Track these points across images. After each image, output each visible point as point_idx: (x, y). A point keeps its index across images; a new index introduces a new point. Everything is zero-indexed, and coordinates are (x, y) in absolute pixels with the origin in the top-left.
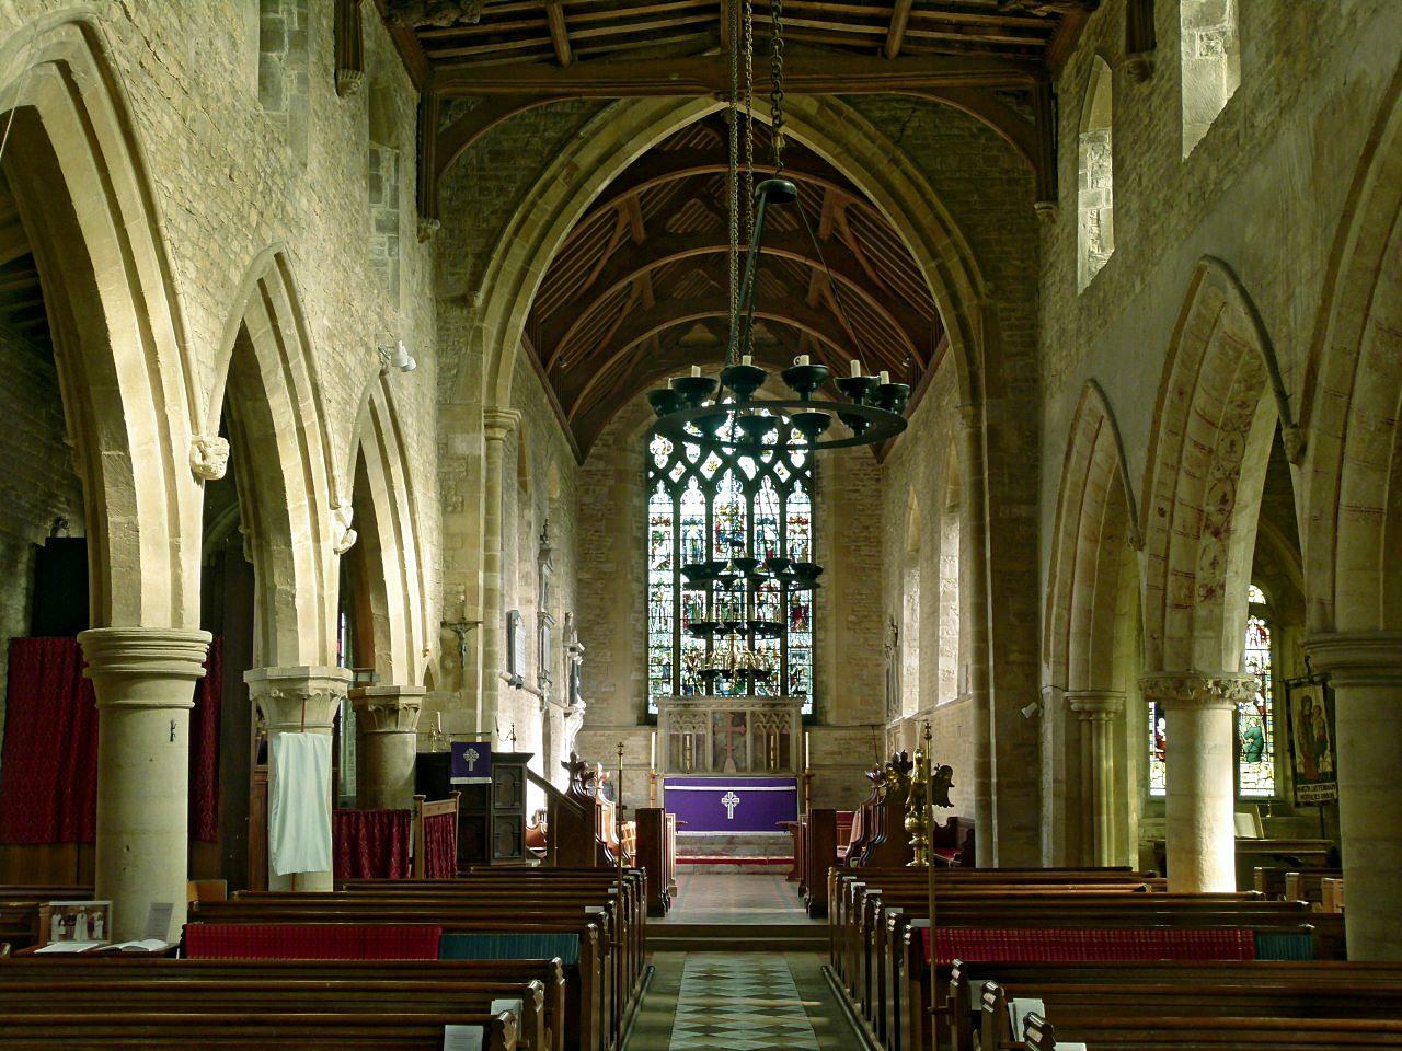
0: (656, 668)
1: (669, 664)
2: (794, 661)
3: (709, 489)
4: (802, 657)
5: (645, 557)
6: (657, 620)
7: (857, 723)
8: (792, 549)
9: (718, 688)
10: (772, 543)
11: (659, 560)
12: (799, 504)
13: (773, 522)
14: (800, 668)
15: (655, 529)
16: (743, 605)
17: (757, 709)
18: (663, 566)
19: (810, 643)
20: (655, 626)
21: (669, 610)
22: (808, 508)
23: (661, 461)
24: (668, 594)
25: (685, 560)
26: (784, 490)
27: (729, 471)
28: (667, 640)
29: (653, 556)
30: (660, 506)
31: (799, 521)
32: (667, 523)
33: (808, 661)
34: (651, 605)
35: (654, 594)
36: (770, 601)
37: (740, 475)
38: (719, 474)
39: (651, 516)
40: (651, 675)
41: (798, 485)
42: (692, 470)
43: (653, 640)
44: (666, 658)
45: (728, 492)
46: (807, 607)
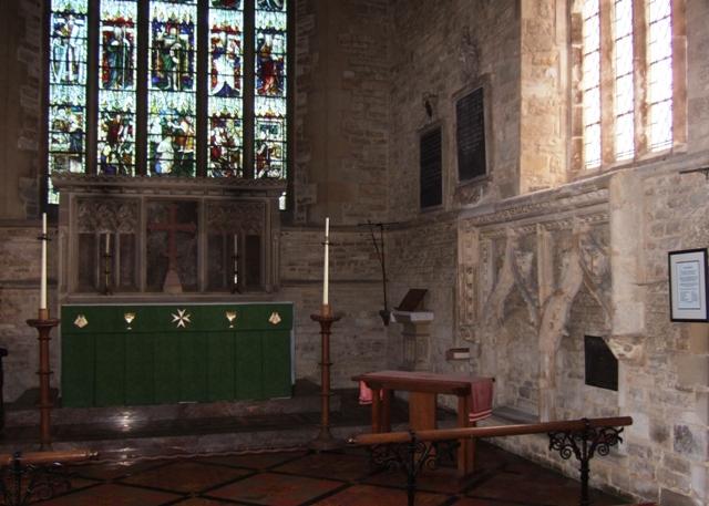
0: (59, 137)
1: (79, 131)
2: (262, 136)
4: (273, 131)
6: (63, 65)
7: (354, 222)
14: (270, 145)
16: (191, 52)
17: (213, 196)
19: (284, 113)
20: (58, 74)
21: (82, 52)
24: (80, 29)
28: (77, 95)
33: (280, 136)
34: (54, 42)
35: (58, 27)
36: (230, 49)
40: (53, 146)
43: (56, 95)
44: (76, 122)
46: (280, 63)
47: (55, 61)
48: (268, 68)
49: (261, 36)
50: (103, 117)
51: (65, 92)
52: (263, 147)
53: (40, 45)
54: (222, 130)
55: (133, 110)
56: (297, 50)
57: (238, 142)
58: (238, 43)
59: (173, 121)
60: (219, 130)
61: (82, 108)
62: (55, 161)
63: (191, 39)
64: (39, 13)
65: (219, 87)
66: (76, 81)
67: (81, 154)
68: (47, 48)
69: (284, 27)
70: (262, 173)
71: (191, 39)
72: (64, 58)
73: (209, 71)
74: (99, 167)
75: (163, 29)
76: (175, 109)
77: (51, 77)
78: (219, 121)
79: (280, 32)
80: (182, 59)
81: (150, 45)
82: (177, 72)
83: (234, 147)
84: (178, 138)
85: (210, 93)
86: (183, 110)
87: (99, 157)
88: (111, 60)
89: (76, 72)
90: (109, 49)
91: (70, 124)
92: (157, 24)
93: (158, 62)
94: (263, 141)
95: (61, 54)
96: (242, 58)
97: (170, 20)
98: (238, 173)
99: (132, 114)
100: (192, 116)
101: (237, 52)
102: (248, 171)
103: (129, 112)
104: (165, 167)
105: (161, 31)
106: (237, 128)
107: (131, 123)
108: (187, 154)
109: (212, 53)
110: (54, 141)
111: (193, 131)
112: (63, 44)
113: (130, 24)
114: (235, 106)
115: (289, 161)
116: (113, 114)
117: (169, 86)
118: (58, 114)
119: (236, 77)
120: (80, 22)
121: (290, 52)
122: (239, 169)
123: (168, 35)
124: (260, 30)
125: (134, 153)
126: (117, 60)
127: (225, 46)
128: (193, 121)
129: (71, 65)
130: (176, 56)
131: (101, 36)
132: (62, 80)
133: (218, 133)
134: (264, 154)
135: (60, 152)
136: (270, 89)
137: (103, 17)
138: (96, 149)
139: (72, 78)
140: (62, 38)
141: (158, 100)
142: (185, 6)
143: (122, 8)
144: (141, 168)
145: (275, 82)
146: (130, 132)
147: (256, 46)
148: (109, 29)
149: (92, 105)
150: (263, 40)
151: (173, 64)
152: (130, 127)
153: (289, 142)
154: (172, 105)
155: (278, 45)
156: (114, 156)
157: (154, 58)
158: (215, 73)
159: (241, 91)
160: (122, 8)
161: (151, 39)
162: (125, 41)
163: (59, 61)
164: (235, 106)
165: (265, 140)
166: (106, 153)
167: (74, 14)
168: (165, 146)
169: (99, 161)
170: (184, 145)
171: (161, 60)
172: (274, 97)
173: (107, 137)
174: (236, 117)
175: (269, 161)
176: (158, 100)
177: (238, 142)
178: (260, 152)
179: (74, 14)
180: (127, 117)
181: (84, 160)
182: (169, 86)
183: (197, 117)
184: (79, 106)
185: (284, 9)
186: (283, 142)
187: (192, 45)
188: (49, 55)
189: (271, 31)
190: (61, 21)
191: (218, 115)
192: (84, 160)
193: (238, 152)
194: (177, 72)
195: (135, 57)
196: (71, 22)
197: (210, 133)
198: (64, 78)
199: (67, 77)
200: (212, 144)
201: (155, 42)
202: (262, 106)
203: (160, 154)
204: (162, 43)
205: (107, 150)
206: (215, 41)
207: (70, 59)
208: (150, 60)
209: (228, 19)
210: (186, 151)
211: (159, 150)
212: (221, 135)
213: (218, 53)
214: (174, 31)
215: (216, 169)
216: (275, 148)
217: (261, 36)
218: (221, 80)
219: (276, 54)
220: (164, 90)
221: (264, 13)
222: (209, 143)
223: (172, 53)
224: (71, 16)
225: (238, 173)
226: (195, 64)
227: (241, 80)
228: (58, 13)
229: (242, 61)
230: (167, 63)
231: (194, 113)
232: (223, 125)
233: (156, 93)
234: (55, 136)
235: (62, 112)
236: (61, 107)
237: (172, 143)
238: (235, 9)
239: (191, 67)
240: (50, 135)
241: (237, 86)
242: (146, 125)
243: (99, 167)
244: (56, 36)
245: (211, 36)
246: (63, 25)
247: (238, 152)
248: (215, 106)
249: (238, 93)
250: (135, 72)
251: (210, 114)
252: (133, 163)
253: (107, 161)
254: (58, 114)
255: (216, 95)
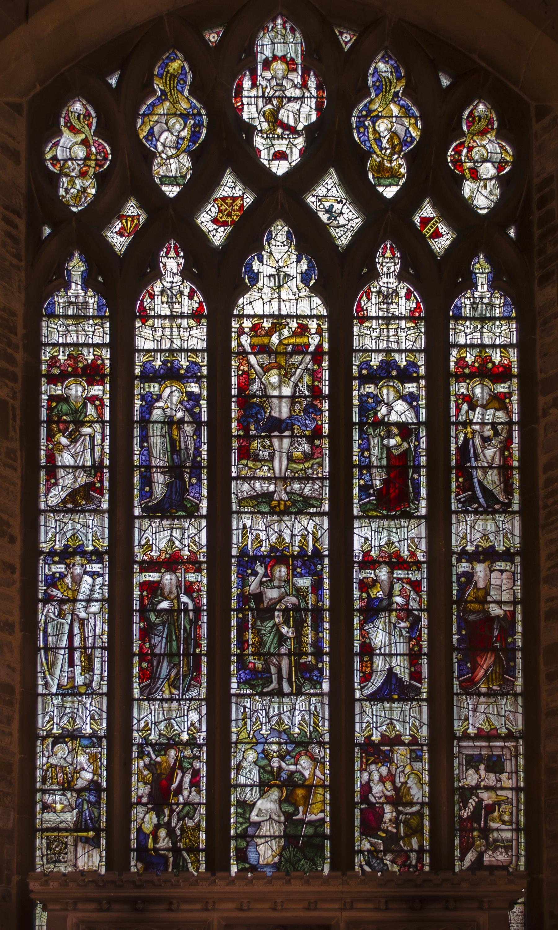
0: (58, 800)
1: (94, 786)
2: (471, 778)
3: (221, 278)
4: (495, 766)
5: (33, 471)
6: (62, 657)
8: (463, 450)
9: (242, 856)
10: (405, 430)
11: (67, 480)
12: (486, 327)
13: (406, 375)
14: (487, 797)
15: (58, 390)
16: (317, 612)
18: (78, 501)
20: (56, 674)
21: (99, 627)
22: (505, 333)
23: (78, 190)
24: (92, 582)
25: (147, 481)
26: (438, 287)
27: (280, 231)
28: (91, 716)
29: (52, 470)
30: (75, 325)
31: (487, 372)
32: (92, 373)
35: (53, 581)
37: (310, 236)
38: (248, 235)
39: (46, 356)
41: (481, 270)
42: (171, 221)
43: (50, 716)
44: (87, 768)
45: (280, 289)
47: (47, 649)
48: (483, 634)
49: (464, 567)
50: (142, 754)
51: (69, 707)
52: (472, 802)
53: (16, 617)
54: (384, 771)
55: (201, 737)
56: (545, 590)
57: (418, 793)
58: (416, 585)
59: (282, 757)
60: (378, 771)
61: (100, 739)
62: (49, 847)
63: (317, 586)
64: (14, 554)
65: (378, 681)
66: (88, 685)
67: (98, 831)
68: (30, 624)
69: (516, 543)
70: (471, 856)
71: (317, 586)
72: (64, 643)
73: (357, 647)
74: (133, 855)
75: (260, 570)
76: (287, 732)
77: (41, 682)
78: (377, 752)
79: (507, 556)
80: (299, 627)
81: (234, 604)
82: (289, 655)
83: (412, 804)
84: (292, 789)
85: (358, 695)
86: (302, 732)
87: (133, 836)
88: (155, 640)
89: (88, 669)
90: (152, 617)
91: (77, 771)
92: (247, 561)
93: (250, 636)
94: (473, 790)
95: (58, 635)
96: (424, 616)
97: (273, 548)
98: (420, 859)
99: (200, 746)
100: (321, 744)
101: (414, 605)
102: (442, 857)
103: (192, 743)
104: (266, 852)
105: (255, 574)
106: (417, 765)
107: (197, 765)
108: (311, 823)
109: (361, 611)
110: (46, 807)
111: (323, 775)
112: (61, 615)
113: (193, 563)
114: (410, 719)
115: (532, 829)
116: (162, 748)
117: (274, 685)
118: (54, 754)
119: (414, 657)
120: (97, 568)
121: (529, 599)
122: (421, 851)
123: (269, 580)
124: (463, 554)
125: (204, 824)
126: (169, 640)
127: (390, 595)
128: (324, 754)
129: (77, 655)
130: (286, 622)
131: (137, 593)
132: (60, 686)
133: (376, 777)
134: (475, 816)
135: (57, 829)
136: (488, 679)
137: (139, 554)
138: (128, 820)
139: (80, 680)
140: (62, 602)
141: (254, 714)
142: (304, 520)
143: (177, 534)
144: (217, 861)
145: (497, 661)
146: (195, 783)
147: (455, 588)
148: (153, 577)
149: (119, 735)
150: (469, 576)
151: (282, 639)
152: (196, 773)
153: (531, 790)
154: (280, 722)
155: (500, 585)
156: (162, 833)
157: (242, 628)
158: (368, 650)
159: (425, 687)
160: (177, 534)
161: (234, 591)
162: (184, 599)
163: (56, 649)
164: (410, 719)
165: (477, 787)
166: (148, 827)
167: (84, 554)
168: (267, 804)
169: (134, 844)
170: (306, 805)
171: (257, 633)
172: (495, 694)
173: (150, 795)
174: (414, 741)
175: (486, 832)
176: (254, 714)
177: (418, 793)
178: (465, 814)
179: (84, 554)
180: (188, 753)
181: (103, 842)
182: (274, 685)
183: (334, 745)
184: (94, 734)
185: (516, 507)
186: (517, 789)
187: (319, 598)
188: (37, 639)
189: (488, 555)
190: (61, 568)
191: (376, 737)
192: (103, 842)
193: (420, 814)
194: (289, 655)
195: (204, 631)
196: (78, 570)
197: (360, 778)
198: (65, 682)
199: (72, 678)
200: (365, 799)
201: (244, 598)
202: (476, 715)
203: (258, 825)
204: (259, 597)
205: (149, 821)
206: (364, 586)
207: (77, 642)
208: (233, 634)
209: (395, 538)
210: (313, 817)
211: (254, 817)
212: (382, 780)
213: (371, 612)
214: (281, 571)
215: (373, 853)
216: (498, 803)
217: (464, 567)
218: (379, 663)
219: (500, 603)
220: (262, 694)
221: (470, 518)
222: (357, 799)
223: (278, 617)
224: (78, 558)
225: (420, 859)
226: (327, 637)
227: (424, 662)
228: (52, 553)
229: (424, 622)
230: (269, 638)
231: (326, 738)
232: (387, 759)
233: (247, 702)
234: (49, 798)
235: (62, 750)
236: (58, 740)
237: (281, 802)
238: (409, 516)
239: (317, 643)
240: (39, 796)
241: (416, 676)
242: (228, 769)
243: (133, 855)
244: (48, 599)
245: (358, 575)
246: (62, 576)
247: (420, 814)
248: (371, 721)
249: (418, 691)
250: (204, 659)
251: (359, 738)
252: (202, 846)
253: (150, 844)
254: (54, 754)
255: (373, 698)
